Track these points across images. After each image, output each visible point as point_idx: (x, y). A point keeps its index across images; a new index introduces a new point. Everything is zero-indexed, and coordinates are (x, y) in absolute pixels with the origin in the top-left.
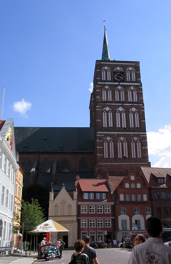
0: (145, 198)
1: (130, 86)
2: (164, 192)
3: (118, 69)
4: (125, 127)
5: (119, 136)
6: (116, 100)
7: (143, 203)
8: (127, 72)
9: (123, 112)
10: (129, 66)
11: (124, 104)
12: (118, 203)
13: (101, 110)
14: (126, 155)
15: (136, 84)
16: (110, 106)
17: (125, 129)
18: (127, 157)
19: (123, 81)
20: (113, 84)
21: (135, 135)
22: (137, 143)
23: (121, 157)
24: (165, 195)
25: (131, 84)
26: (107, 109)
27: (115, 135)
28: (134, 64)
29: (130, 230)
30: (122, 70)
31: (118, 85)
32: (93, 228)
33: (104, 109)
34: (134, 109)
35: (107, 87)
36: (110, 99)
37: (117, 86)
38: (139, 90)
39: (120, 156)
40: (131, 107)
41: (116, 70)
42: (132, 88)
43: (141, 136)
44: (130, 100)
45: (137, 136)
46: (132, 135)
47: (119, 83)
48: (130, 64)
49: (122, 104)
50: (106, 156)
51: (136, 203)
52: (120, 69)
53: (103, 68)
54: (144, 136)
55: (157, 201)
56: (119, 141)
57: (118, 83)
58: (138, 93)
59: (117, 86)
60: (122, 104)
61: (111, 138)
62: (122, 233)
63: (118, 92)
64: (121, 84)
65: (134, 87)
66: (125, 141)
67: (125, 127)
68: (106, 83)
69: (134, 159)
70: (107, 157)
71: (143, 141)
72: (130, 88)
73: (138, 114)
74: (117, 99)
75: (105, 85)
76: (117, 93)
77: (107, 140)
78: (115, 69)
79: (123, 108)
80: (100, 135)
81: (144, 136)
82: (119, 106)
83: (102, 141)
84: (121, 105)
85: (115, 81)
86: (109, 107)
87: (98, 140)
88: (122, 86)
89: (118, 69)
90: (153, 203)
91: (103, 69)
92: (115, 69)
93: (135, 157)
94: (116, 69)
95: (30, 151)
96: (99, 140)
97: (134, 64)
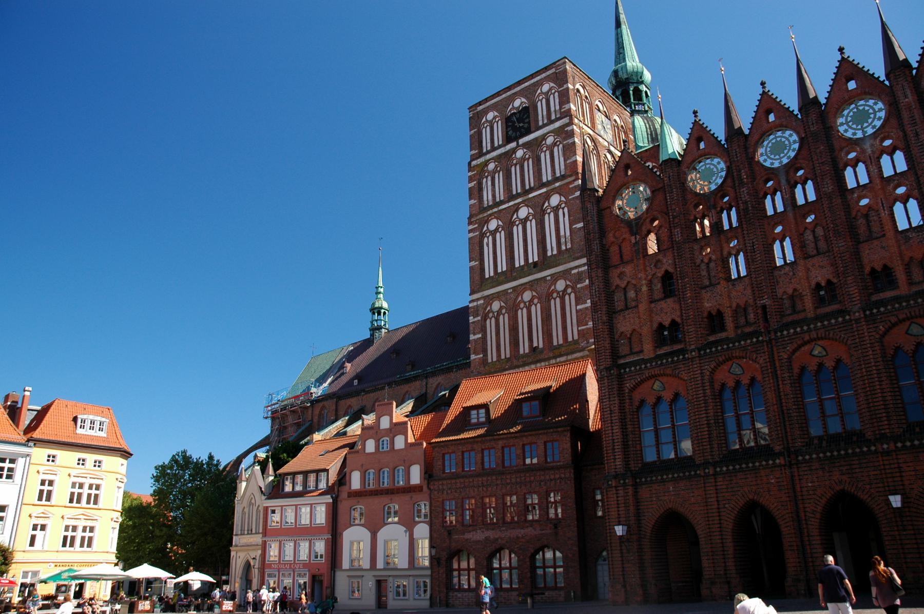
0: (416, 476)
1: (544, 137)
2: (469, 451)
3: (517, 103)
4: (536, 259)
5: (518, 290)
6: (514, 193)
7: (410, 490)
8: (539, 100)
9: (531, 218)
10: (540, 84)
11: (531, 196)
12: (344, 495)
13: (478, 233)
14: (539, 342)
15: (557, 124)
16: (498, 216)
17: (535, 264)
18: (541, 346)
19: (528, 132)
20: (503, 151)
21: (555, 278)
22: (567, 297)
23: (527, 351)
24: (447, 463)
25: (545, 132)
26: (493, 224)
27: (509, 291)
28: (553, 70)
29: (369, 567)
30: (525, 103)
31: (516, 148)
32: (287, 564)
33: (485, 228)
34: (555, 200)
35: (491, 166)
36: (500, 195)
37: (514, 151)
38: (565, 139)
39: (524, 348)
40: (547, 196)
41: (513, 108)
42: (550, 140)
43: (574, 272)
44: (546, 176)
45: (565, 274)
46: (549, 278)
47: (518, 143)
48: (544, 75)
49: (525, 198)
50: (492, 356)
51: (392, 492)
52: (522, 103)
53: (484, 119)
54: (580, 269)
55: (445, 482)
56: (522, 305)
57: (513, 145)
58: (563, 147)
59: (514, 151)
60: (525, 198)
61: (502, 303)
62: (348, 576)
63: (518, 167)
64: (521, 141)
65: (554, 136)
66: (536, 301)
67: (536, 259)
68: (488, 157)
69: (559, 346)
70: (495, 359)
71: (579, 286)
72: (544, 142)
73: (566, 210)
74: (516, 187)
75: (486, 163)
76: (515, 171)
77: (492, 311)
78: (509, 109)
79: (528, 206)
80: (475, 304)
81: (580, 269)
82: (516, 209)
83: (479, 318)
84: (520, 203)
85: (508, 140)
86: (495, 218)
87: (472, 317)
88: (525, 145)
89: (517, 103)
90: (432, 488)
91: (484, 124)
92: (509, 109)
93: (561, 342)
94: (511, 107)
95: (411, 375)
96: (474, 318)
97: (553, 70)
